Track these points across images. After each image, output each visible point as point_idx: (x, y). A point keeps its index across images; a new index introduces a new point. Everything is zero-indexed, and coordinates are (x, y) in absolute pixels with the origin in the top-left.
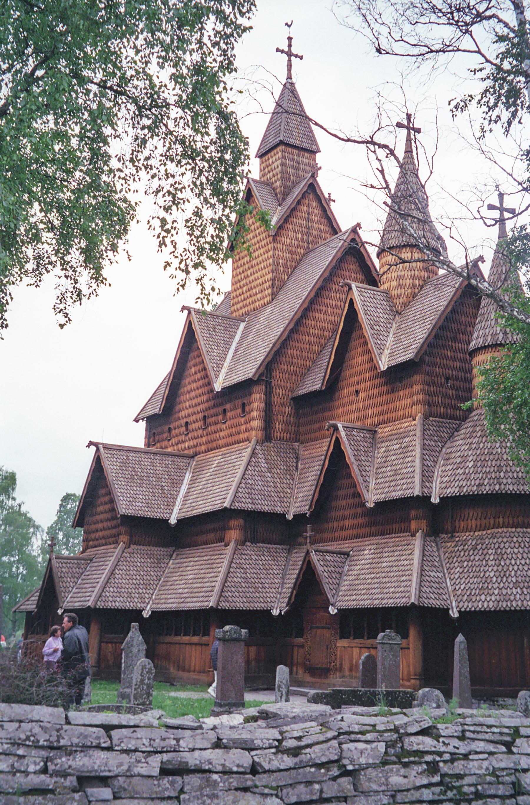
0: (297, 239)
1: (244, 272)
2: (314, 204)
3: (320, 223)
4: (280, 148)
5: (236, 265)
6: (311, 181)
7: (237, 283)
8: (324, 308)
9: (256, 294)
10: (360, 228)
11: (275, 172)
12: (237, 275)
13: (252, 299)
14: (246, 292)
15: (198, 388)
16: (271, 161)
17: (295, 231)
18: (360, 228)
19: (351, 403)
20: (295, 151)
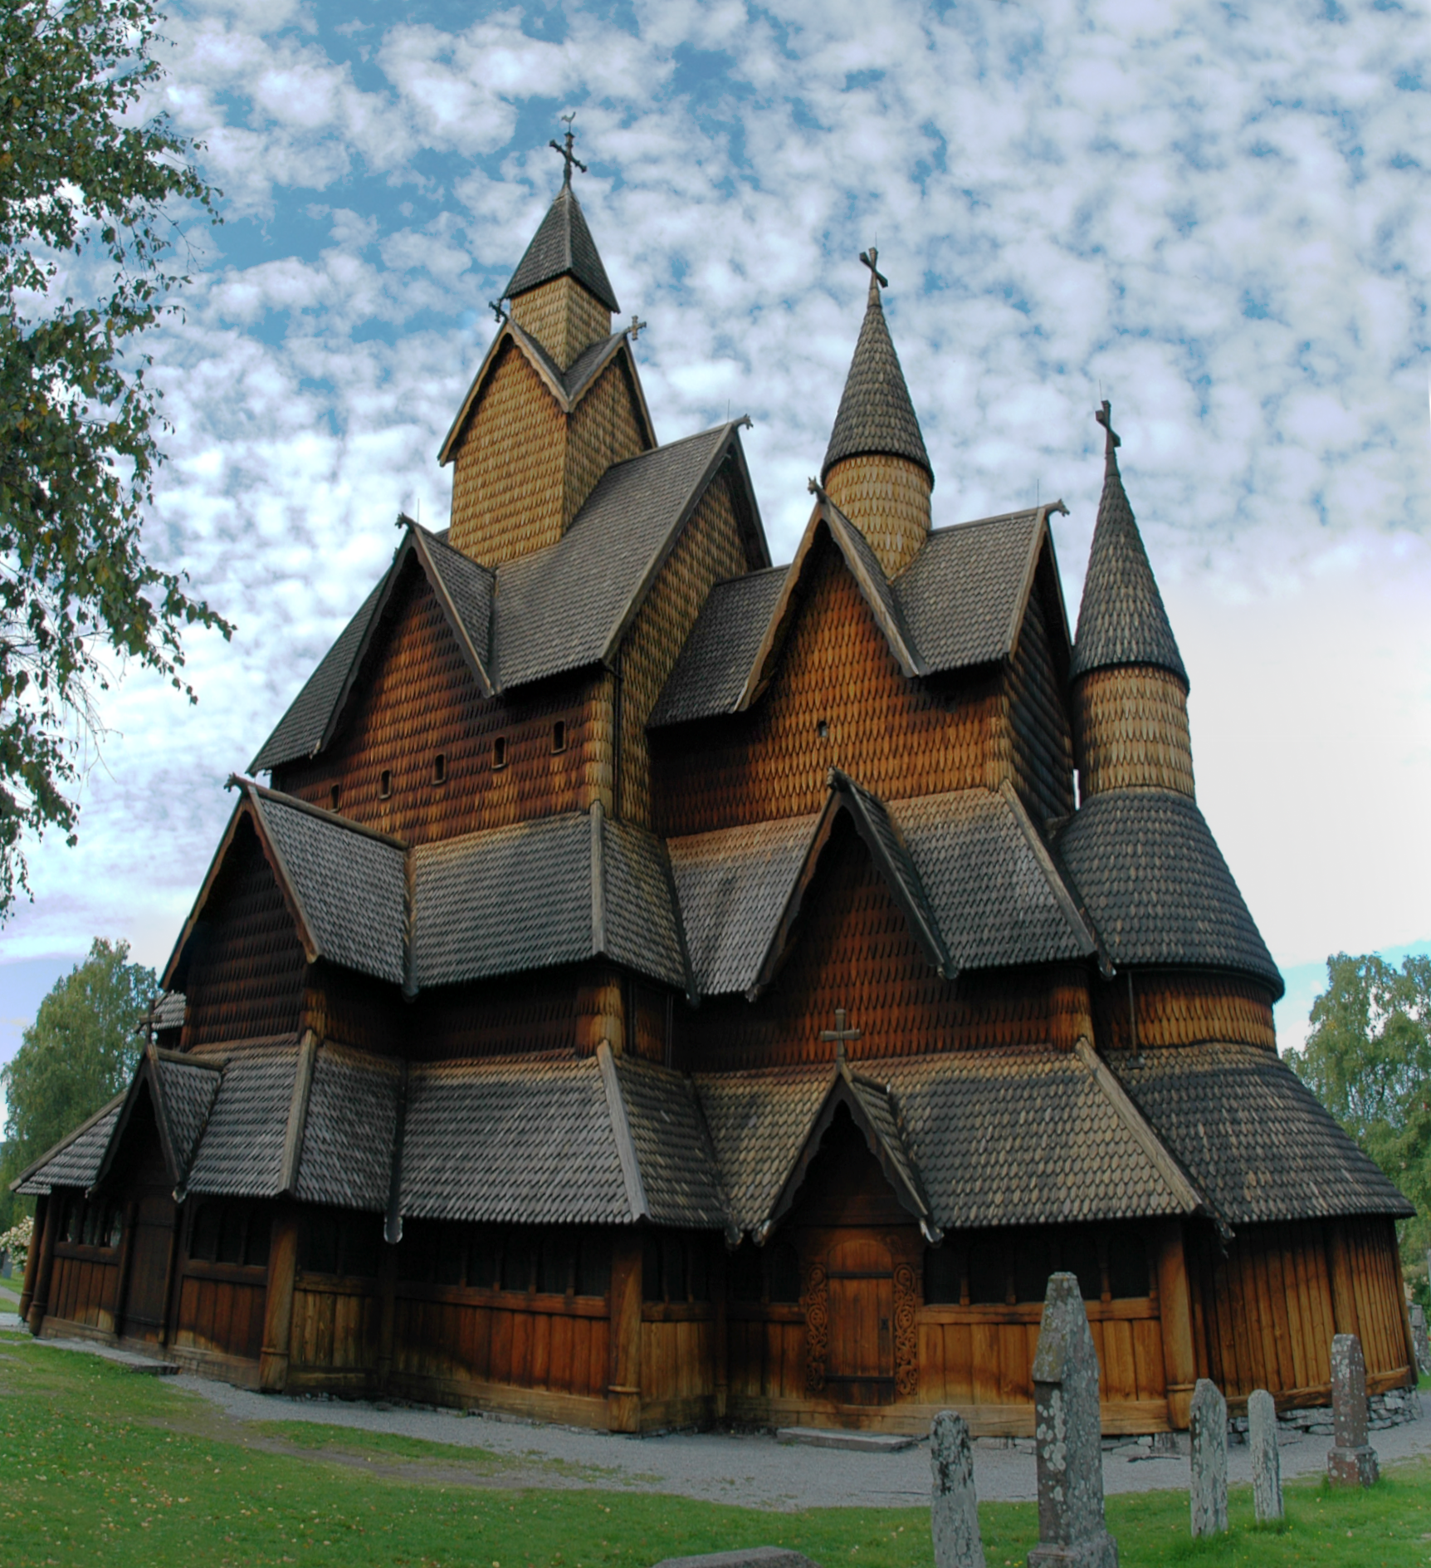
0: (597, 437)
1: (484, 485)
2: (621, 387)
3: (627, 422)
4: (565, 280)
5: (463, 474)
6: (622, 344)
7: (467, 506)
8: (688, 558)
9: (518, 526)
10: (749, 425)
11: (551, 319)
12: (466, 493)
13: (506, 537)
14: (491, 523)
15: (421, 695)
16: (539, 302)
17: (594, 421)
18: (749, 425)
19: (809, 749)
20: (585, 295)
